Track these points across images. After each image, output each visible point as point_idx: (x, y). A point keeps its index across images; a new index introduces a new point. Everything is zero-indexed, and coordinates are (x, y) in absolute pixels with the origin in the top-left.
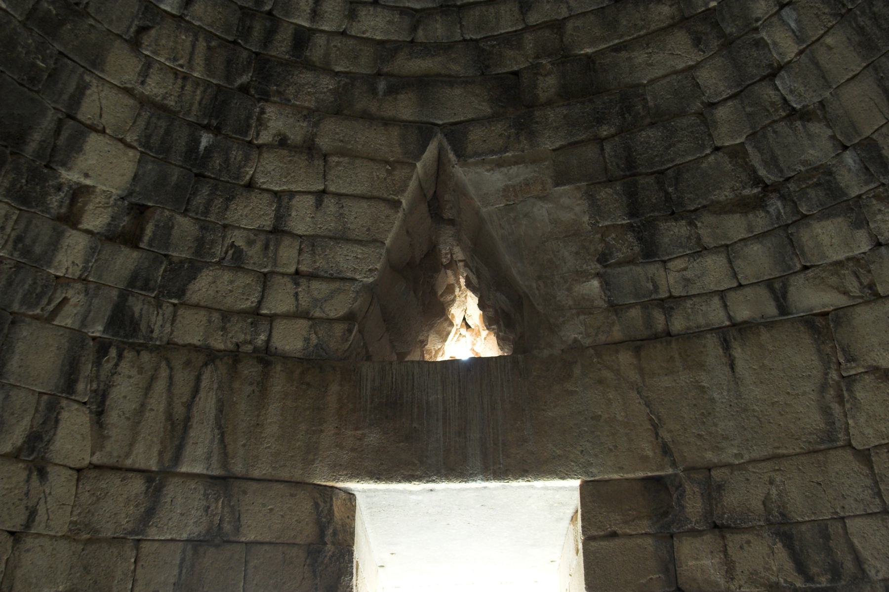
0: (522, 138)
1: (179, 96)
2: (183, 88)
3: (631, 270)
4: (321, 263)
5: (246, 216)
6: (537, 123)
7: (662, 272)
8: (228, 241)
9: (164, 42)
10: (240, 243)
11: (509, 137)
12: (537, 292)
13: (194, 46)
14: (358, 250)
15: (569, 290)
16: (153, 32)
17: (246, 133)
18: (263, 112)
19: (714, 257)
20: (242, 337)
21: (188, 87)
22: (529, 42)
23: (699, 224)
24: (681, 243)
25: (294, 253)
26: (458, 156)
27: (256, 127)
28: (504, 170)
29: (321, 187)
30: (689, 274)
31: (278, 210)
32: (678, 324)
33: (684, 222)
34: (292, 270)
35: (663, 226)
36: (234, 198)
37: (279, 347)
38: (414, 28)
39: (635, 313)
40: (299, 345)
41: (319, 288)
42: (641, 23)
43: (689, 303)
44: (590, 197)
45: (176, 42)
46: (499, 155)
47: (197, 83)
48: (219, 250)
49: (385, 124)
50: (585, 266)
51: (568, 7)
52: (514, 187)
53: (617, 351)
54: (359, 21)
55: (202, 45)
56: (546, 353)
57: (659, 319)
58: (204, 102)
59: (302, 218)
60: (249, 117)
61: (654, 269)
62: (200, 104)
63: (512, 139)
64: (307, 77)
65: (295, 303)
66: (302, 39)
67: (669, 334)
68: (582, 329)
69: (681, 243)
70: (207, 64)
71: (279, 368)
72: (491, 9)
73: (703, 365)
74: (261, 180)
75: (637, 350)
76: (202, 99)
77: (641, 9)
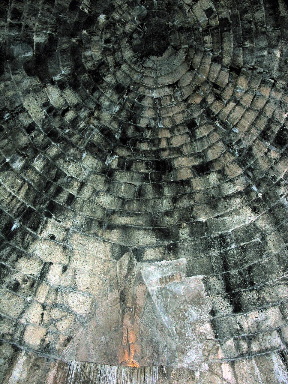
0: (171, 255)
1: (9, 203)
2: (12, 200)
3: (227, 318)
4: (59, 301)
5: (26, 267)
6: (179, 248)
7: (245, 321)
8: (14, 277)
9: (9, 178)
10: (20, 280)
11: (164, 254)
12: (175, 332)
13: (22, 186)
14: (81, 298)
15: (194, 330)
16: (6, 173)
17: (35, 229)
18: (46, 222)
19: (273, 309)
20: (7, 331)
21: (14, 201)
22: (176, 215)
23: (263, 293)
24: (254, 302)
25: (46, 292)
26: (138, 261)
27: (42, 228)
28: (162, 269)
29: (66, 262)
30: (260, 319)
31: (43, 270)
32: (255, 347)
33: (255, 292)
34: (42, 300)
35: (244, 294)
36: (22, 256)
37: (27, 342)
38: (123, 204)
39: (230, 342)
40: (38, 342)
41: (56, 313)
42: (228, 206)
43: (261, 335)
44: (206, 281)
45: (15, 181)
46: (159, 262)
47: (18, 201)
48: (7, 280)
49: (104, 241)
50: (202, 317)
51: (195, 201)
52: (166, 278)
53: (221, 364)
54: (99, 197)
55: (26, 187)
56: (179, 365)
57: (244, 345)
58: (20, 209)
59: (54, 276)
60: (40, 222)
61: (239, 317)
62: (18, 209)
63: (166, 255)
64: (71, 214)
65: (41, 319)
66: (71, 199)
67: (249, 353)
68: (201, 352)
69: (254, 302)
70: (26, 195)
71: (23, 353)
72: (160, 201)
73: (272, 371)
74: (38, 253)
75: (232, 364)
76: (19, 208)
77: (228, 200)
